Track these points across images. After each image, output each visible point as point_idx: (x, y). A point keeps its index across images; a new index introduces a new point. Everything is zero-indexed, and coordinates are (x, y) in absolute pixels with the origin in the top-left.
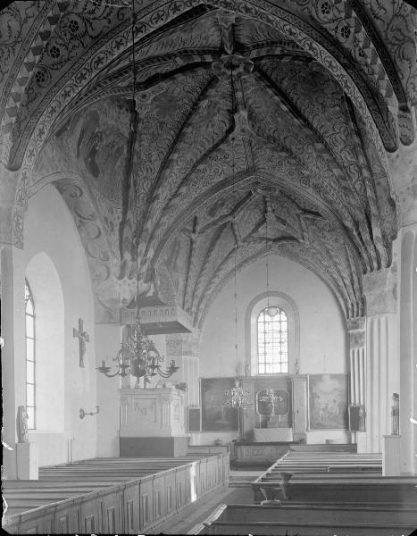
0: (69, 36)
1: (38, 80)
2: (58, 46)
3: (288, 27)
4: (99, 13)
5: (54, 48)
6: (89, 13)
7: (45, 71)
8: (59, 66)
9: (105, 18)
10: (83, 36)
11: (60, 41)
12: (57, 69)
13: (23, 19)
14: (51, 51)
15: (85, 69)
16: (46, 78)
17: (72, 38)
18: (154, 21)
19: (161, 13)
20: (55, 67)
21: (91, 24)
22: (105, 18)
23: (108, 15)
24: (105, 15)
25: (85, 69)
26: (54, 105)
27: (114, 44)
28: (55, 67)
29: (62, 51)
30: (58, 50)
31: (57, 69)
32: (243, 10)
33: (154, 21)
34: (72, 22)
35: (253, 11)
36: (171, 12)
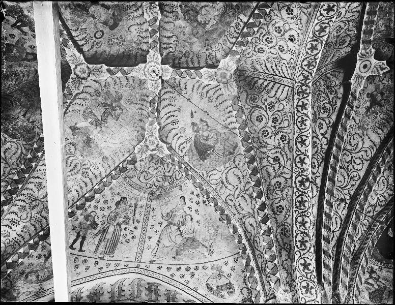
0: (279, 193)
1: (285, 235)
2: (279, 204)
3: (322, 12)
4: (283, 163)
5: (277, 207)
6: (279, 169)
7: (285, 225)
9: (287, 161)
10: (286, 183)
11: (277, 201)
12: (289, 216)
13: (252, 213)
16: (288, 229)
17: (282, 191)
18: (304, 127)
19: (300, 119)
20: (287, 216)
21: (284, 173)
22: (287, 161)
23: (287, 158)
24: (286, 160)
25: (298, 197)
26: (299, 238)
27: (299, 165)
28: (287, 216)
29: (283, 203)
30: (280, 206)
31: (289, 216)
32: (315, 52)
33: (304, 127)
34: (275, 185)
35: (314, 43)
36: (304, 111)
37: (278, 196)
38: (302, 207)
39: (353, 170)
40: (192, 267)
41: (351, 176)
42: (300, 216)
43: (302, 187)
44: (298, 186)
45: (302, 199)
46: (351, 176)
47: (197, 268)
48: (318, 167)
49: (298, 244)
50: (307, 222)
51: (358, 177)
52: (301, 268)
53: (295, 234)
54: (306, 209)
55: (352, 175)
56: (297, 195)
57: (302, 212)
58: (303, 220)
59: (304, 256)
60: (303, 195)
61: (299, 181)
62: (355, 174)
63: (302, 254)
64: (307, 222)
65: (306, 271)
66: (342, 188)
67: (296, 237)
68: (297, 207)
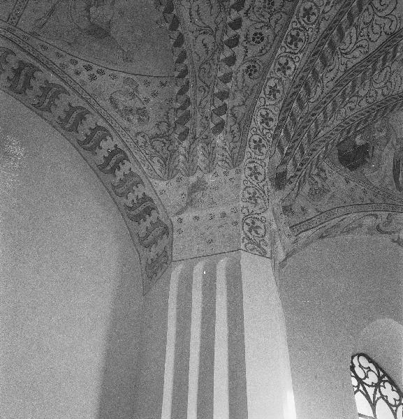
2: (258, 31)
8: (268, 48)
14: (253, 40)
15: (294, 29)
16: (258, 68)
17: (271, 15)
25: (294, 29)
30: (261, 34)
37: (262, 19)
38: (293, 46)
39: (366, 37)
40: (95, 68)
41: (358, 44)
42: (286, 56)
43: (305, 19)
44: (301, 14)
45: (298, 35)
46: (358, 44)
47: (101, 72)
48: (332, 6)
49: (267, 90)
50: (289, 68)
51: (366, 50)
52: (259, 119)
53: (268, 76)
54: (296, 52)
55: (361, 43)
56: (294, 26)
57: (290, 52)
58: (287, 63)
59: (268, 107)
60: (301, 31)
61: (305, 10)
62: (364, 43)
63: (267, 103)
64: (289, 68)
65: (264, 125)
66: (342, 53)
67: (269, 79)
68: (286, 42)
